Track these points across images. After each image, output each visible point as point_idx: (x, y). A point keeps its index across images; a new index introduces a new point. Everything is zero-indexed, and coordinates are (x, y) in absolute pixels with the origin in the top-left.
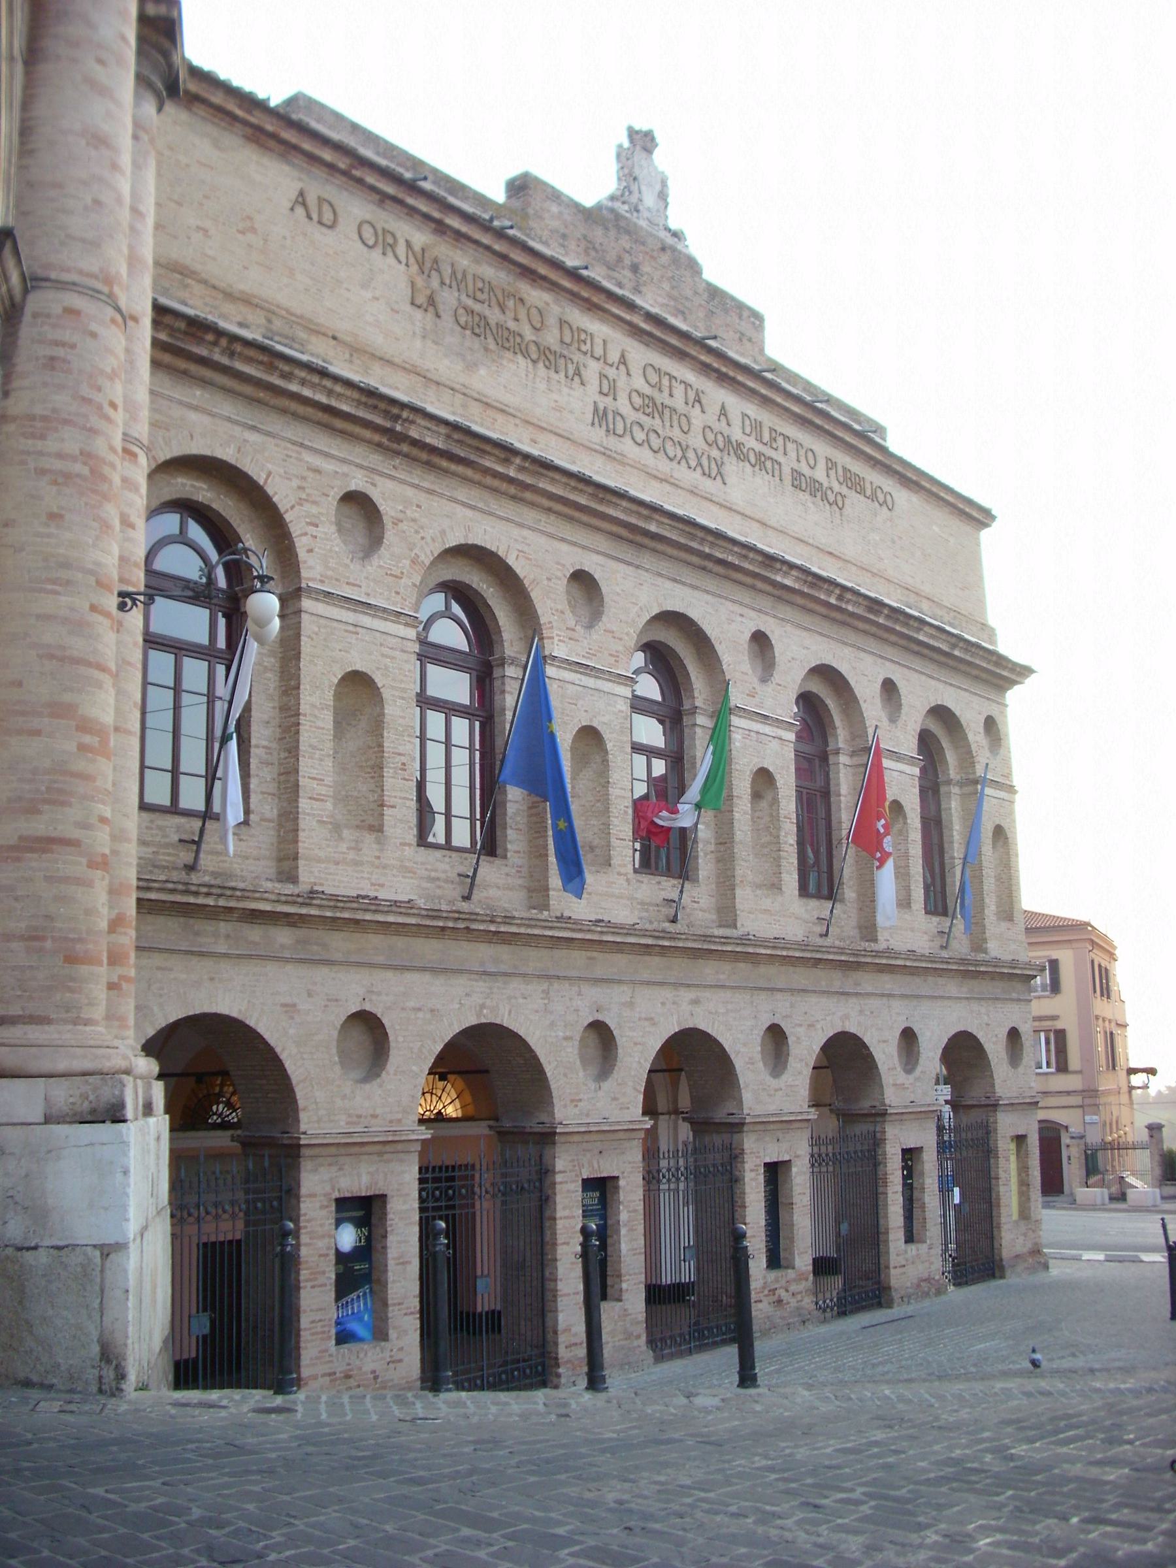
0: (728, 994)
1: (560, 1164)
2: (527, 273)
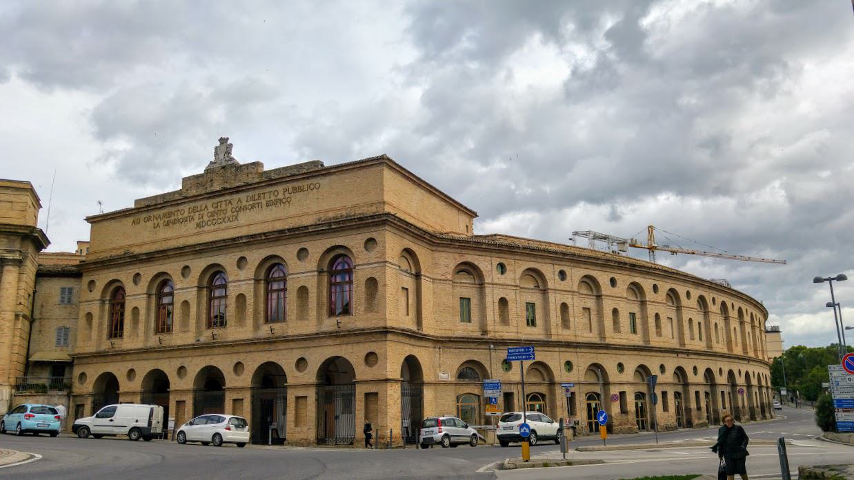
0: (222, 356)
1: (170, 397)
2: (178, 204)
